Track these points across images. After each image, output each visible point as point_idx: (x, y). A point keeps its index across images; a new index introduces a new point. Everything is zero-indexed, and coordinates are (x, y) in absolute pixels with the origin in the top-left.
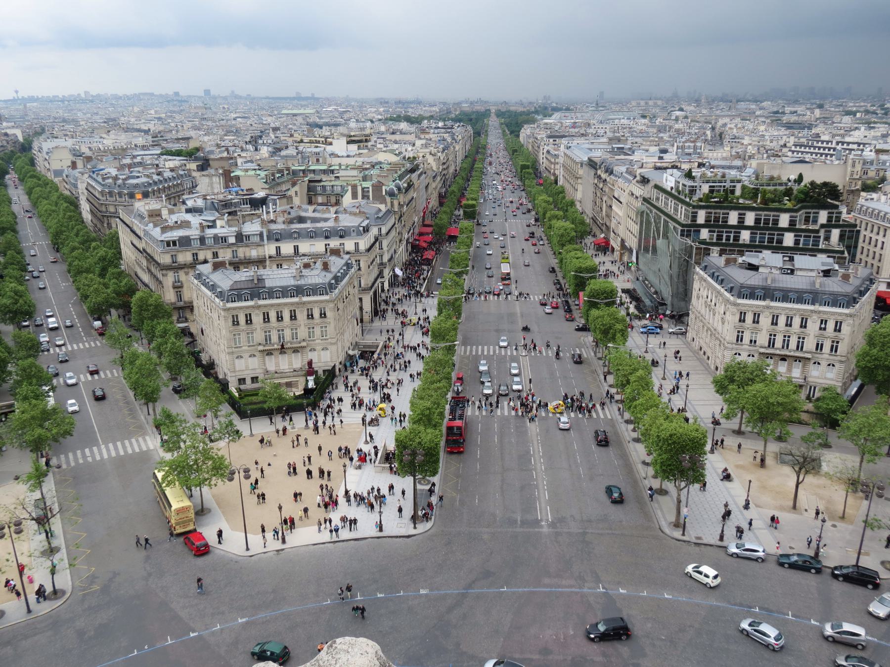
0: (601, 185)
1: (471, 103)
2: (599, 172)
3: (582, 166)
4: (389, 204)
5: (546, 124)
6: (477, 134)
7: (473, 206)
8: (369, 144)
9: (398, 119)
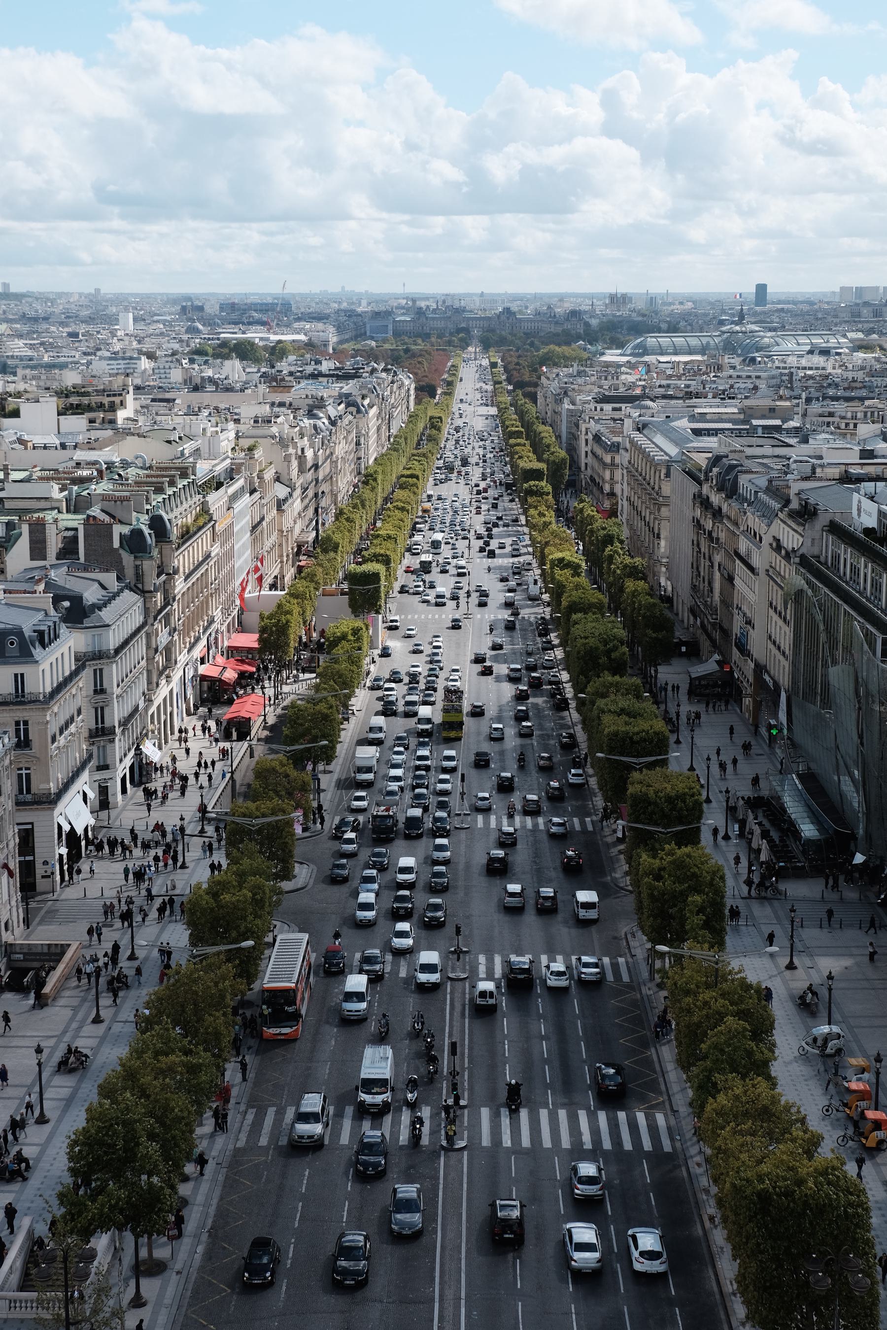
0: (709, 524)
1: (420, 312)
2: (705, 489)
3: (668, 475)
4: (130, 572)
6: (426, 390)
7: (374, 577)
8: (121, 415)
9: (227, 350)
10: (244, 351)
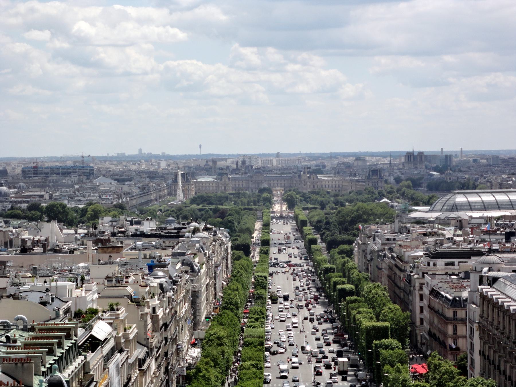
1: (222, 173)
5: (419, 222)
10: (57, 214)
